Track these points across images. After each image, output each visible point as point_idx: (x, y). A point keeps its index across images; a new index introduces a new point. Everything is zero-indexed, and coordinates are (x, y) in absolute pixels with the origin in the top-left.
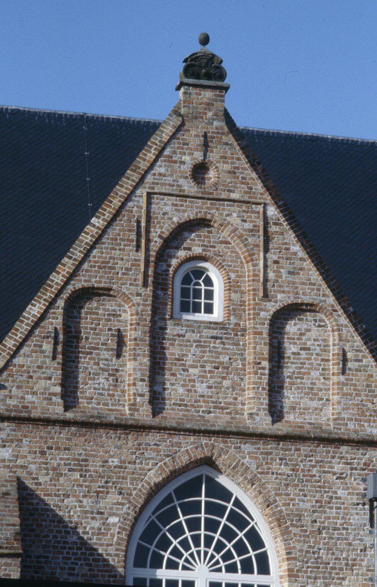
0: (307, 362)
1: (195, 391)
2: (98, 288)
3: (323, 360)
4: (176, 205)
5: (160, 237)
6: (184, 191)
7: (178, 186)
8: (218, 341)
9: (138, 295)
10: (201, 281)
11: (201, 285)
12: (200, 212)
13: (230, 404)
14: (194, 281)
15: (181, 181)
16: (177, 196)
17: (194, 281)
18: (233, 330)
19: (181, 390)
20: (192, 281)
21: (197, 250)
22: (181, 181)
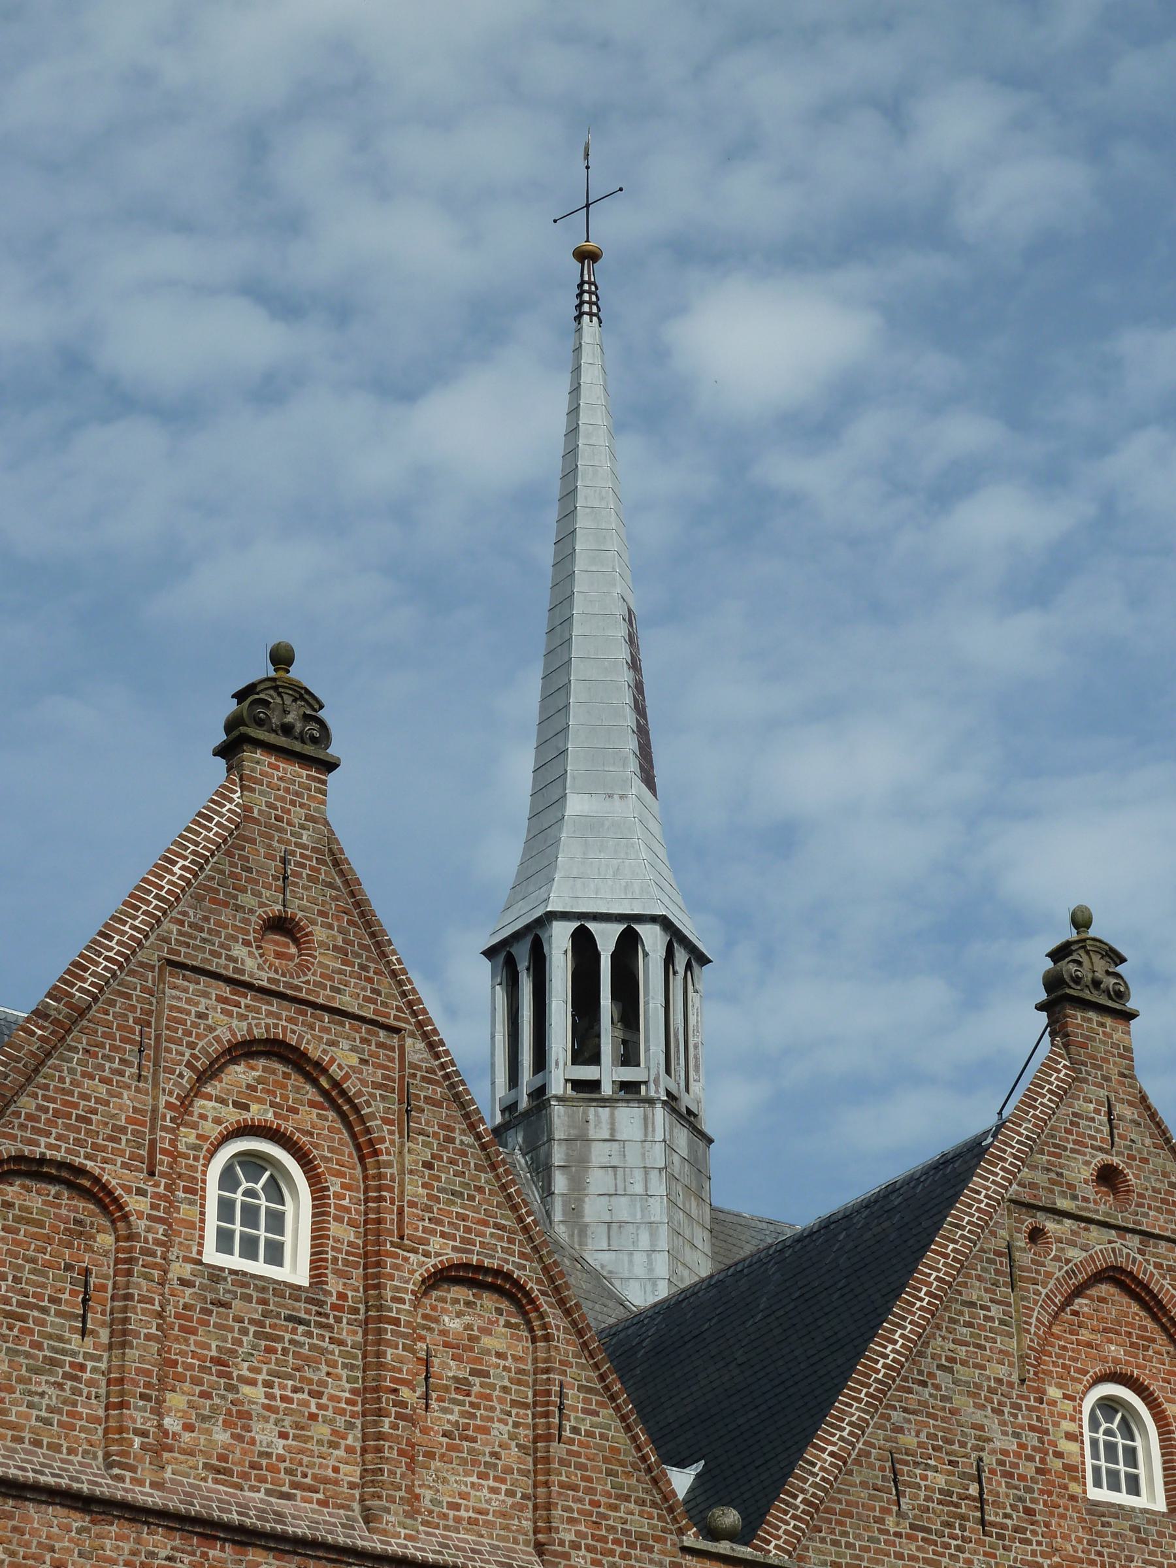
0: (483, 1403)
1: (253, 1442)
2: (52, 1162)
3: (514, 1403)
4: (225, 1000)
5: (189, 1065)
6: (242, 972)
7: (230, 958)
8: (301, 1328)
9: (141, 1192)
10: (259, 1187)
11: (258, 1198)
12: (276, 1026)
13: (326, 1481)
14: (245, 1185)
15: (239, 951)
16: (229, 981)
17: (245, 1185)
18: (334, 1307)
19: (222, 1437)
20: (239, 1184)
21: (259, 1113)
22: (239, 951)
